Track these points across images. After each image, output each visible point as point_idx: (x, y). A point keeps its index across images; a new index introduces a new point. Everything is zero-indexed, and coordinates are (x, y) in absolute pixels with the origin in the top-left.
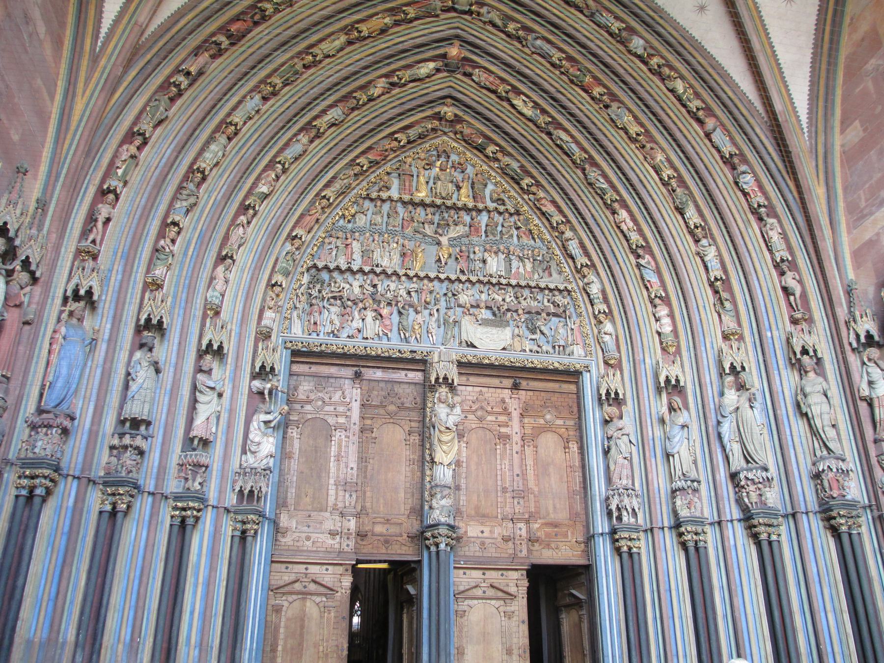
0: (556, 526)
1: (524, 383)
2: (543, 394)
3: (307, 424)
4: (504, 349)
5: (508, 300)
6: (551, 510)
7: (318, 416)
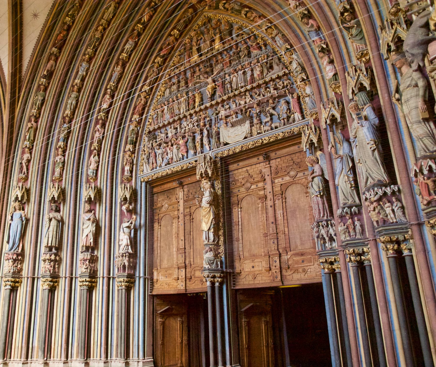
0: (302, 255)
1: (272, 155)
2: (287, 157)
3: (163, 219)
4: (245, 138)
5: (248, 101)
6: (298, 243)
7: (166, 213)
